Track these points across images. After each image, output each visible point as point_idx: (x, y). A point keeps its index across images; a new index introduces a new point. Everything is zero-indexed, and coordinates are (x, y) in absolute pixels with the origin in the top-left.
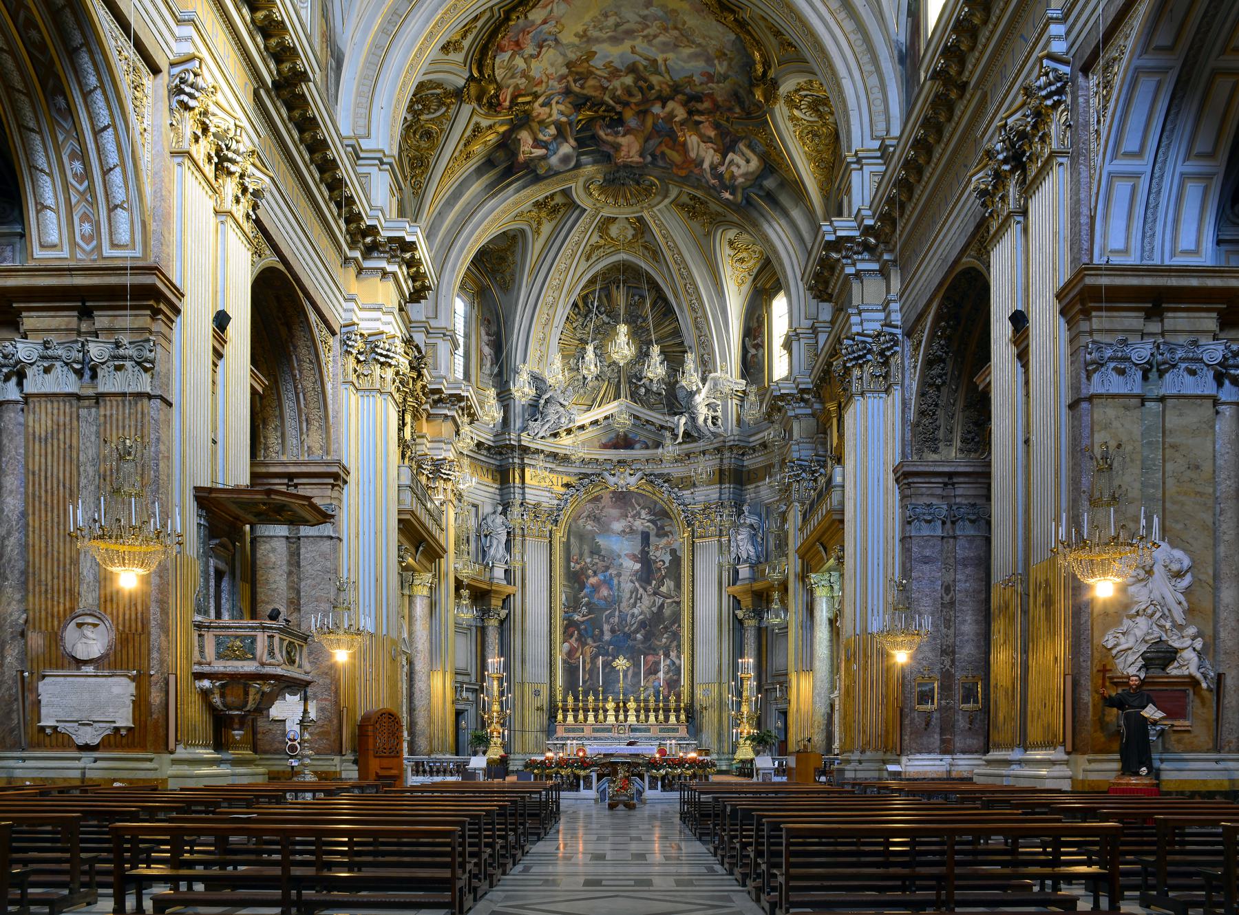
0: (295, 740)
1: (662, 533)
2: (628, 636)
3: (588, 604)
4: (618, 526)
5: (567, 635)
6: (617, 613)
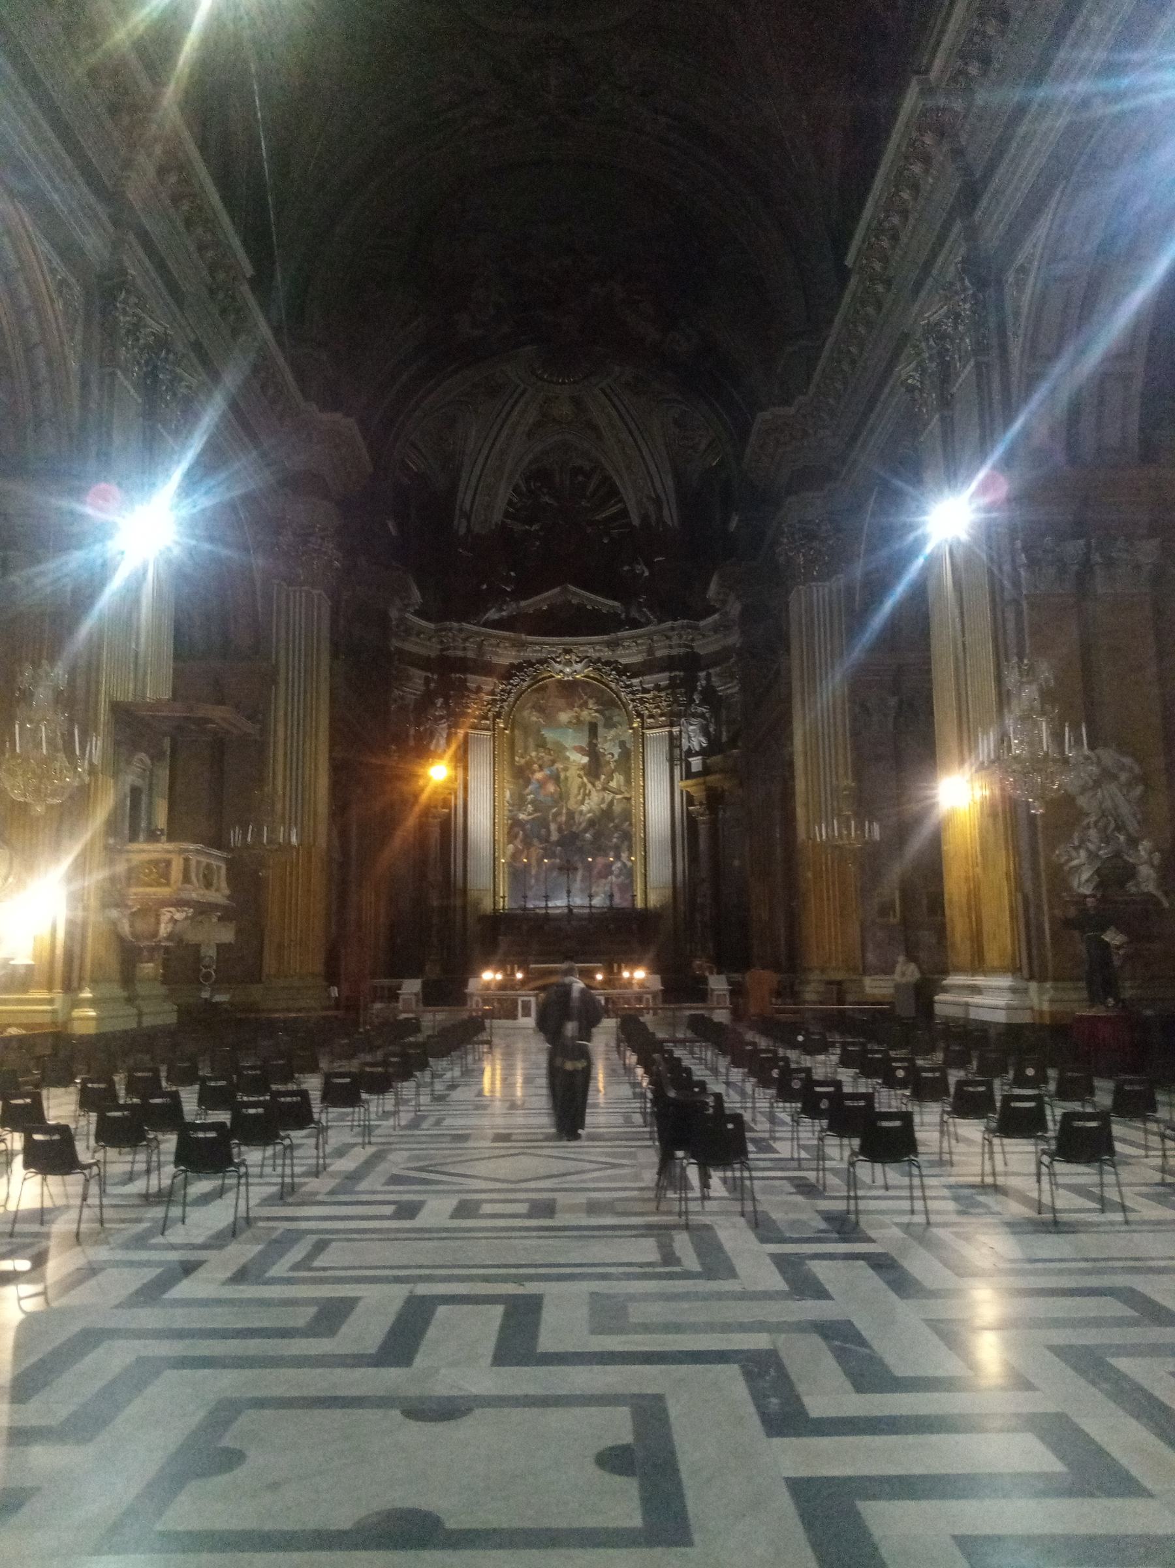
0: (210, 967)
1: (609, 724)
2: (574, 837)
3: (532, 802)
4: (564, 717)
5: (511, 837)
6: (564, 811)
